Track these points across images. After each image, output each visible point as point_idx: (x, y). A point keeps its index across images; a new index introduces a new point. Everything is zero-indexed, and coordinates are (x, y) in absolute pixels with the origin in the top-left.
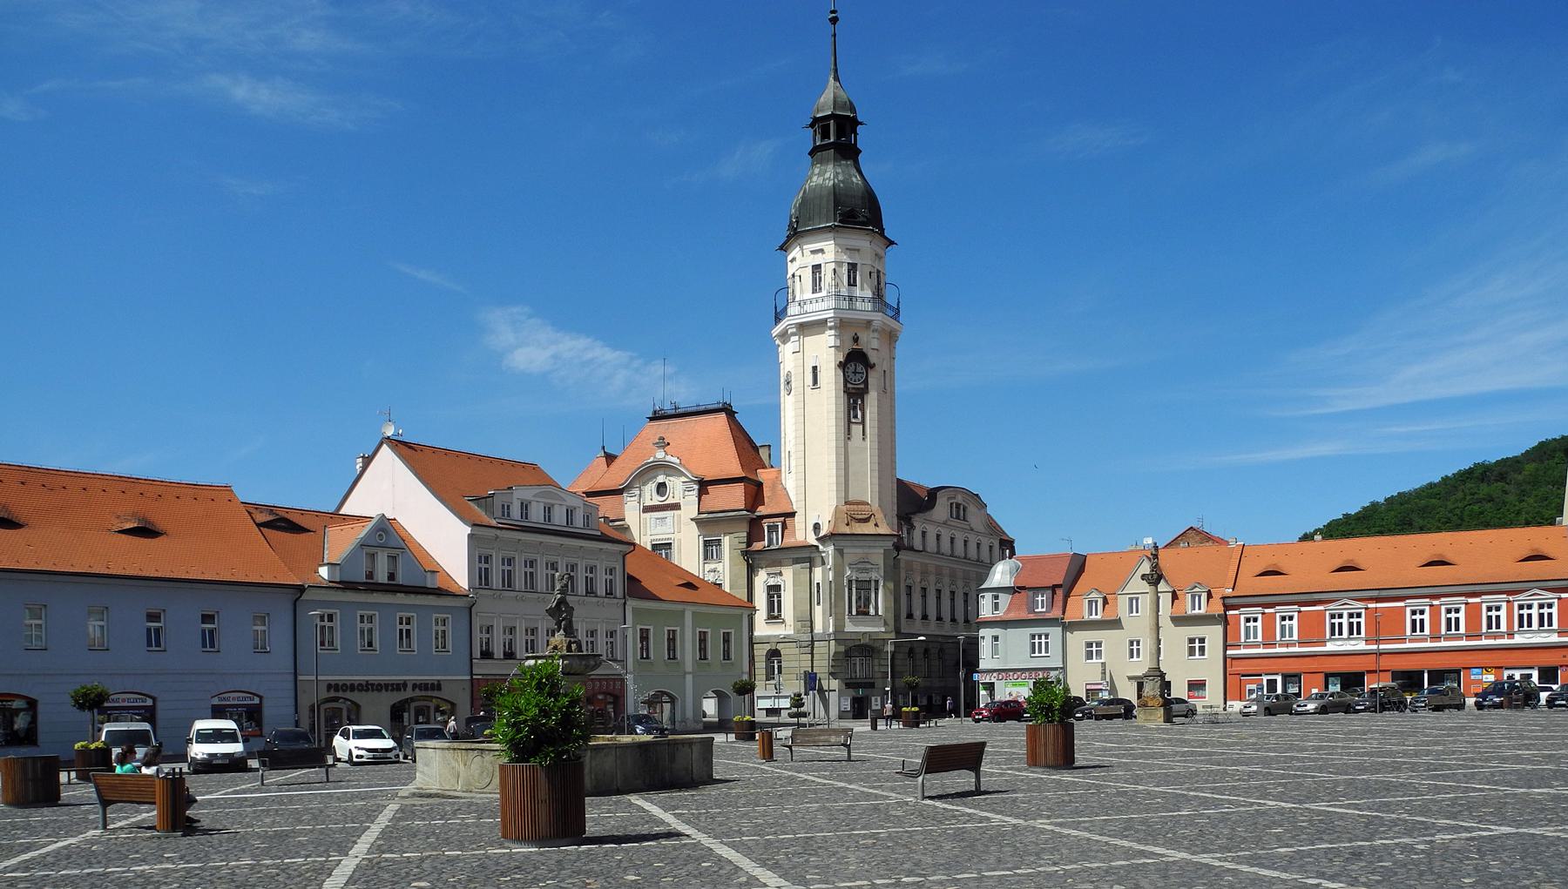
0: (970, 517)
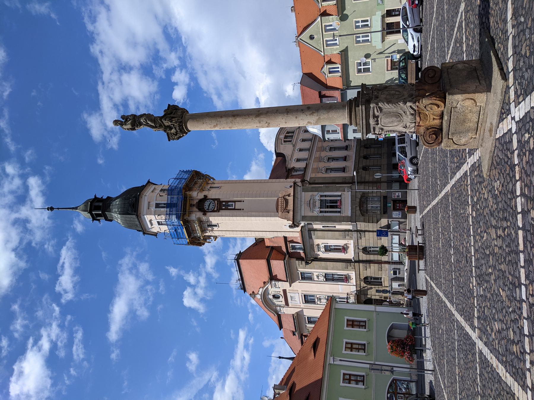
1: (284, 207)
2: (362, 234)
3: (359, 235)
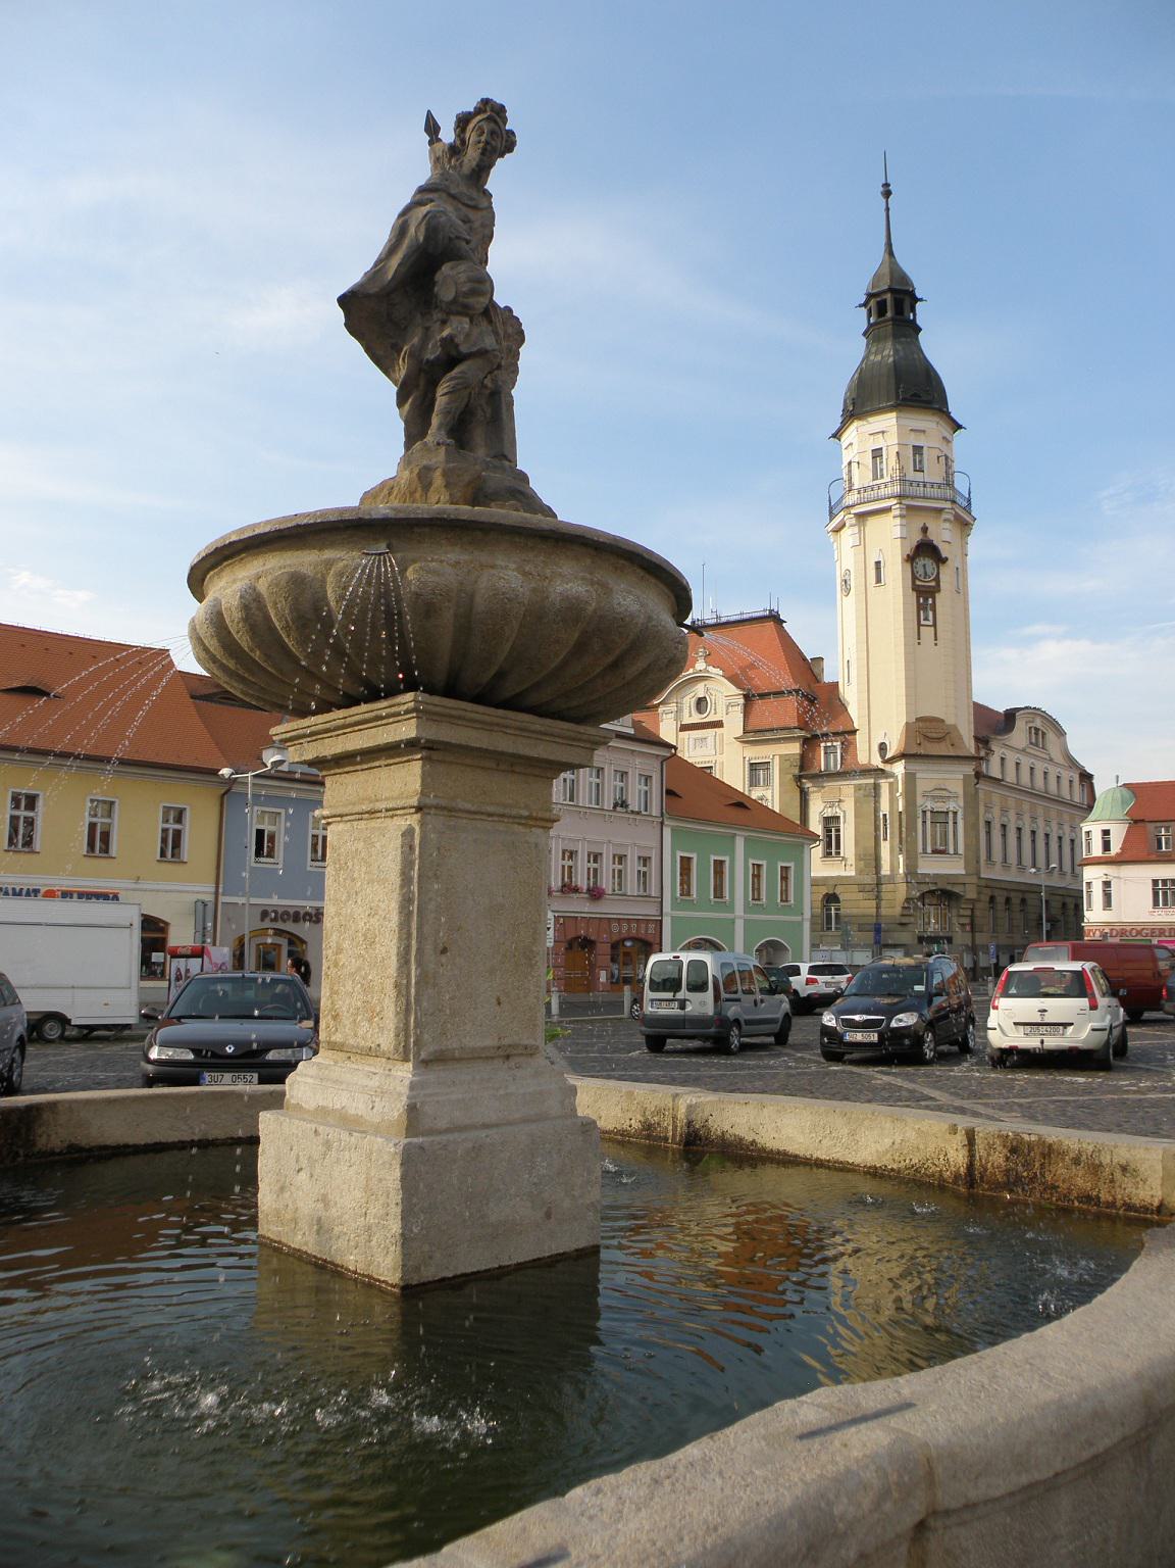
0: (1049, 746)
1: (929, 735)
2: (872, 895)
3: (868, 888)
